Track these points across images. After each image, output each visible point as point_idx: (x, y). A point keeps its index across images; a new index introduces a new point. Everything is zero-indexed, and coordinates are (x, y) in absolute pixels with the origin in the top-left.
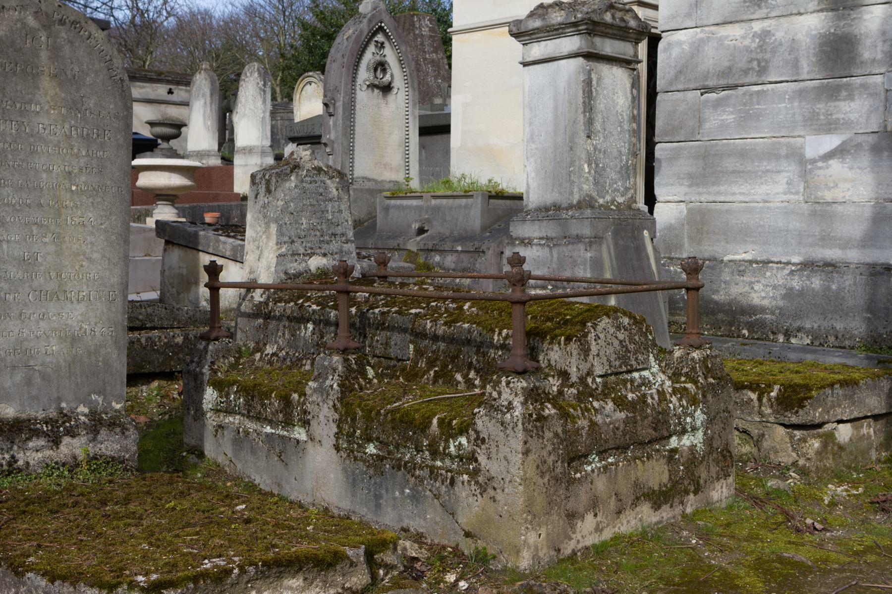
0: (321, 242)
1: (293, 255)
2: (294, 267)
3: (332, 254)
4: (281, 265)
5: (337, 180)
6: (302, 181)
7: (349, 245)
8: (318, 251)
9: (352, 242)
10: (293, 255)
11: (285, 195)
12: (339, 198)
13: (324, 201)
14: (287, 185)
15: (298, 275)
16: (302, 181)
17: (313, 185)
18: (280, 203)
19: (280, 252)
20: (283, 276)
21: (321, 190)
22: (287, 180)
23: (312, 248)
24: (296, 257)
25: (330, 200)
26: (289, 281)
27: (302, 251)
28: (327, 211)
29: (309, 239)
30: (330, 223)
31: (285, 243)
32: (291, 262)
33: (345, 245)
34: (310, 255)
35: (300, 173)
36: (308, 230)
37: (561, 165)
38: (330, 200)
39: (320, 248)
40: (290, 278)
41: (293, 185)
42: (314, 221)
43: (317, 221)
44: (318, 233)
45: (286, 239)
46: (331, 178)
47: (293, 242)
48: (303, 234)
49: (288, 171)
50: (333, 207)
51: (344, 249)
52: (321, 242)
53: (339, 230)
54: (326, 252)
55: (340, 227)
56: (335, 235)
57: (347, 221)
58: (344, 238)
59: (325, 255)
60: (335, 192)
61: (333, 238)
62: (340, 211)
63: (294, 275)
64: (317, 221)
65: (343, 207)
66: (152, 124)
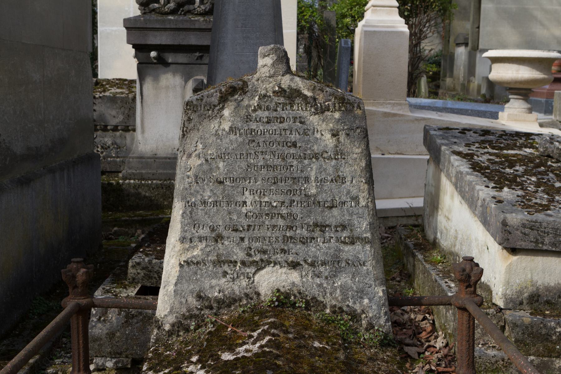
0: (286, 239)
1: (219, 262)
2: (217, 286)
3: (312, 265)
4: (189, 281)
5: (337, 115)
6: (248, 119)
7: (358, 247)
8: (279, 257)
9: (365, 241)
10: (219, 262)
11: (205, 147)
12: (339, 153)
13: (301, 158)
14: (214, 125)
15: (228, 302)
16: (248, 119)
17: (275, 126)
18: (195, 162)
19: (189, 255)
20: (193, 302)
21: (294, 137)
22: (210, 118)
23: (264, 252)
24: (226, 268)
25: (316, 156)
26: (207, 312)
27: (239, 255)
28: (307, 179)
29: (257, 233)
30: (311, 202)
31: (201, 239)
32: (215, 276)
33: (347, 248)
34: (260, 266)
35: (246, 102)
36: (258, 216)
37: (100, 80)
38: (316, 156)
39: (283, 251)
40: (211, 308)
41: (226, 126)
42: (275, 199)
43: (281, 198)
44: (281, 222)
45: (203, 232)
46: (321, 111)
47: (219, 238)
48: (245, 222)
49: (215, 100)
50: (321, 170)
51: (344, 256)
52: (286, 239)
53: (334, 216)
54: (300, 260)
55: (335, 211)
56: (323, 227)
57: (355, 199)
58: (345, 234)
59: (294, 265)
60: (328, 141)
61: (317, 233)
62: (339, 179)
63: (220, 302)
64: (281, 198)
65: (346, 171)
66: (445, 227)
